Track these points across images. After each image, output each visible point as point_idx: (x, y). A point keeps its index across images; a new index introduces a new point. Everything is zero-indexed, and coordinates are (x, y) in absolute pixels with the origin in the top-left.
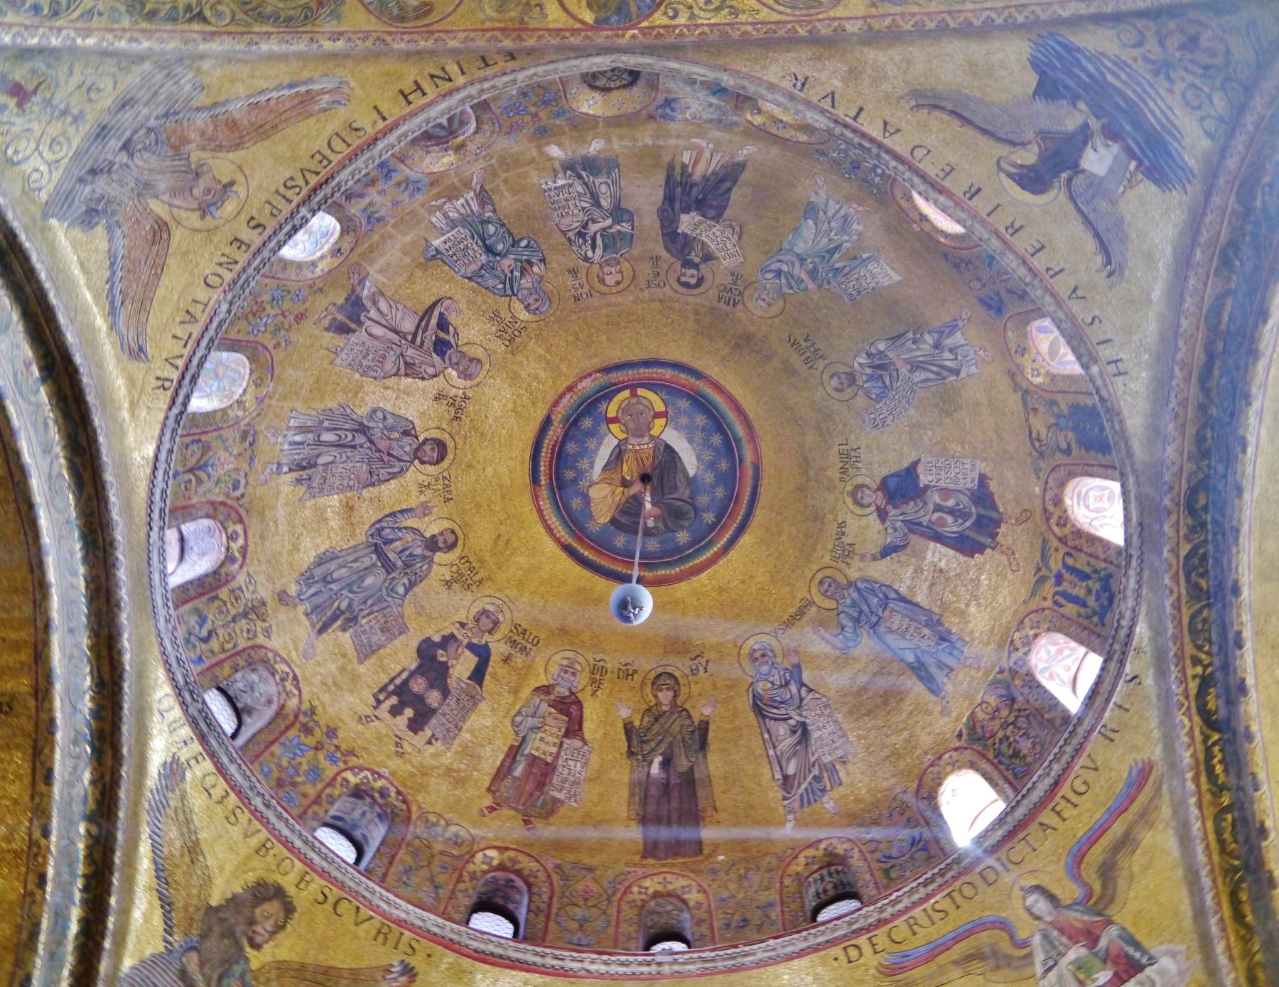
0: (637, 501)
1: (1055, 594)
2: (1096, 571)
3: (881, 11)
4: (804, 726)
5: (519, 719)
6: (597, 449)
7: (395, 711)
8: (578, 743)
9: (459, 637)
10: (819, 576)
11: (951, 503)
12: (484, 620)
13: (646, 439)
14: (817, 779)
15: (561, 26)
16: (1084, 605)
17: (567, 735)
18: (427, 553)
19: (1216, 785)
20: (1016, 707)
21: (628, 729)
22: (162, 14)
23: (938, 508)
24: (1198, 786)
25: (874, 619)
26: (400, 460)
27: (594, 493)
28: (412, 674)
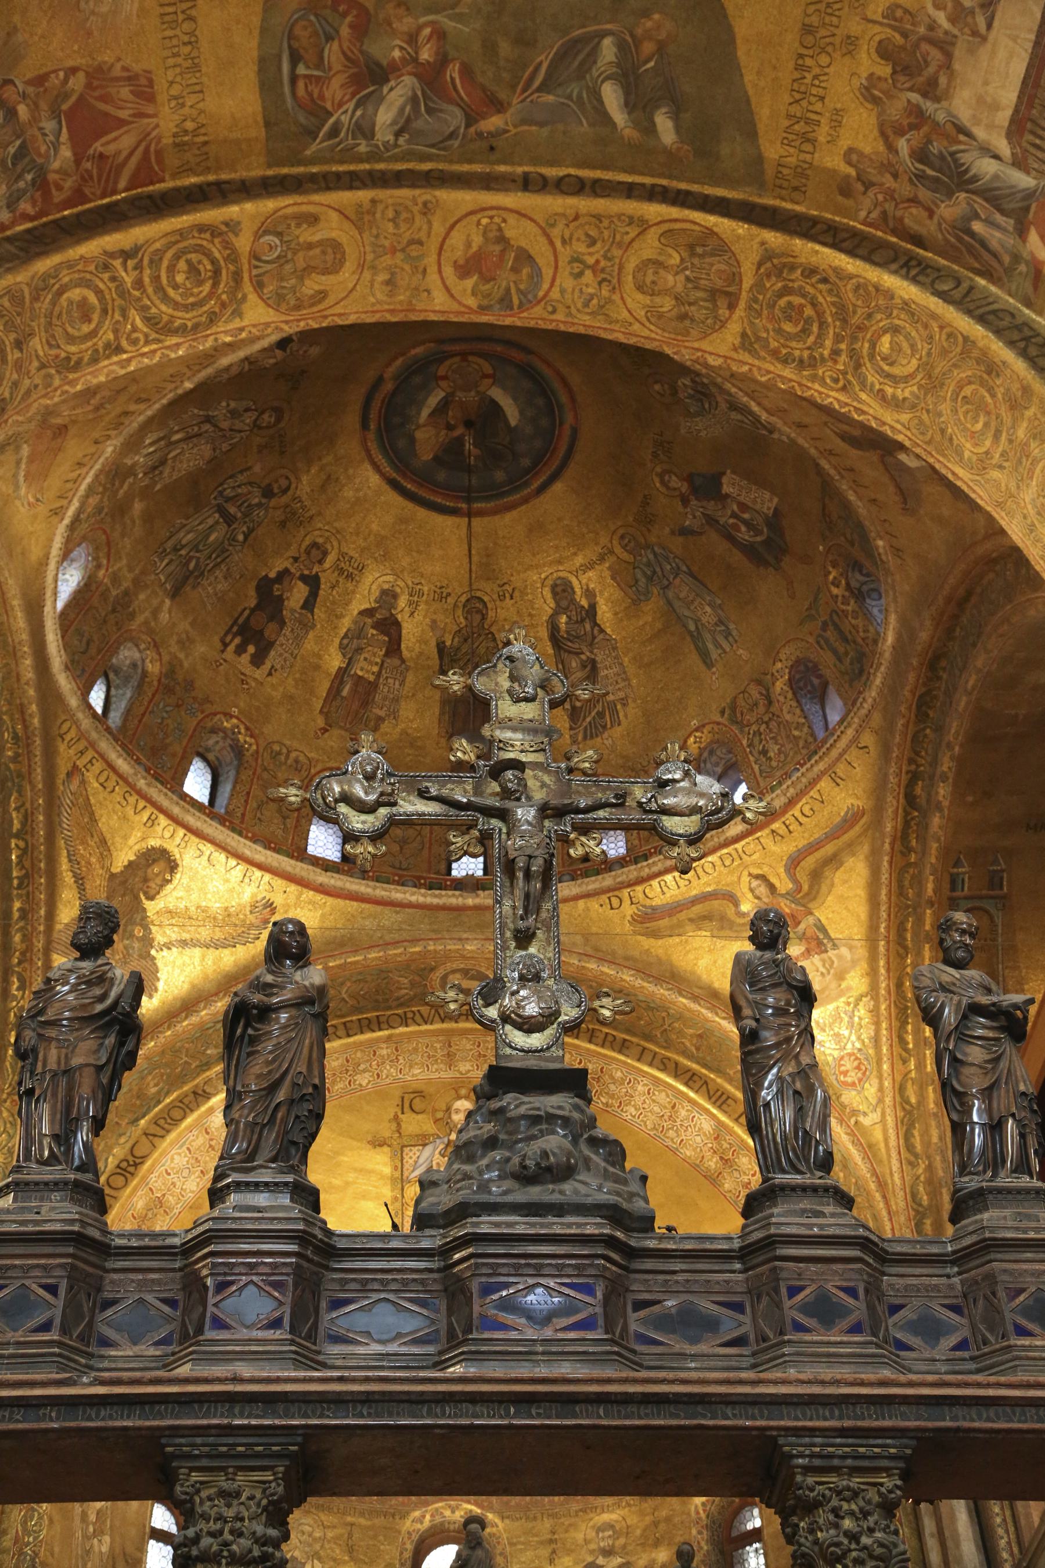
0: (460, 441)
1: (820, 636)
2: (854, 642)
3: (741, 358)
4: (593, 662)
5: (345, 641)
6: (426, 399)
7: (240, 650)
8: (396, 662)
9: (293, 570)
10: (621, 531)
11: (746, 516)
12: (314, 552)
13: (473, 393)
14: (601, 715)
15: (446, 309)
16: (840, 660)
17: (387, 654)
18: (264, 501)
19: (907, 848)
20: (772, 709)
21: (441, 648)
22: (86, 359)
23: (734, 515)
24: (892, 849)
25: (666, 583)
26: (240, 431)
27: (419, 435)
28: (253, 611)
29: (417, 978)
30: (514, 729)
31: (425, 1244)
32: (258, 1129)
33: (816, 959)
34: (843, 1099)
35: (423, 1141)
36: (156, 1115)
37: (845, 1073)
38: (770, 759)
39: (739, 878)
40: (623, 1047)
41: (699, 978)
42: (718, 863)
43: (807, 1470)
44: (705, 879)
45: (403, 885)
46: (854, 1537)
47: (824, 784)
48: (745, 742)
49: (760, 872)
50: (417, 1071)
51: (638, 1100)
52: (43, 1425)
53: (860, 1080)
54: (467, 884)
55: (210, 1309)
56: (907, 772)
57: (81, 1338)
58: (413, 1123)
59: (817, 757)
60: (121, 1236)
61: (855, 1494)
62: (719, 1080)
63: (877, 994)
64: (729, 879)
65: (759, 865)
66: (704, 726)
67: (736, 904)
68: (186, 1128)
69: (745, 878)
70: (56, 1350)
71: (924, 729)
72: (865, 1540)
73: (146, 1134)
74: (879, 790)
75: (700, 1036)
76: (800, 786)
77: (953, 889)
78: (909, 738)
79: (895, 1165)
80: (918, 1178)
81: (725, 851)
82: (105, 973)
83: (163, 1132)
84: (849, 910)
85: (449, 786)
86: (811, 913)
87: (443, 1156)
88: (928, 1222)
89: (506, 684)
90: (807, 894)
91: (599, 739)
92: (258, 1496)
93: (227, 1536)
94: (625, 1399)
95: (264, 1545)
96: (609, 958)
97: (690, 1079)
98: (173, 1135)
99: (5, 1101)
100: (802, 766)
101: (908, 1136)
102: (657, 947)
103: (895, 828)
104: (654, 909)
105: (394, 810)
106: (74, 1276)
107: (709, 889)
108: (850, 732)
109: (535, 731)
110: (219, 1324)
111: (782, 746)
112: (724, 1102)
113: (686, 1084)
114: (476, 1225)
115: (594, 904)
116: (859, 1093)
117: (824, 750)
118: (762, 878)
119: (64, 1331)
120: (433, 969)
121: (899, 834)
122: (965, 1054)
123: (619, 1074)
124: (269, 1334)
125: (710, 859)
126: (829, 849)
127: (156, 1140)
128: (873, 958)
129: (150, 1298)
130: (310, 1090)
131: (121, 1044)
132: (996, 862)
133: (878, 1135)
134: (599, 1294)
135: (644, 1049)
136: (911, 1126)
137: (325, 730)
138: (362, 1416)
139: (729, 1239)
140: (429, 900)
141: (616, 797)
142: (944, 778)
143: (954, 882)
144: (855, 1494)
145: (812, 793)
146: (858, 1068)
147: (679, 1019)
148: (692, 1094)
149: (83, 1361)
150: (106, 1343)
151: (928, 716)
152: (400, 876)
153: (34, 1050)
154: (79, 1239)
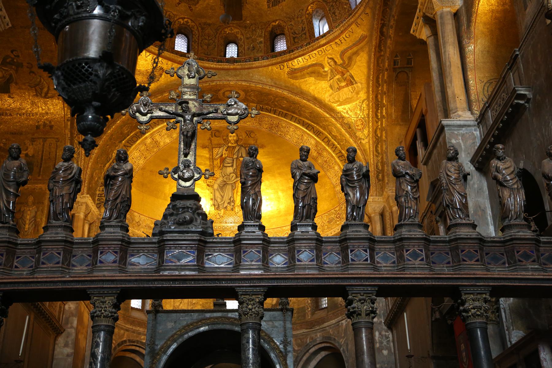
24: (375, 50)
29: (215, 93)
30: (187, 88)
31: (154, 240)
32: (112, 210)
33: (350, 87)
34: (357, 134)
35: (219, 146)
36: (128, 139)
37: (358, 126)
38: (336, 16)
39: (324, 59)
40: (285, 116)
41: (310, 93)
42: (317, 53)
43: (241, 295)
44: (312, 59)
45: (208, 61)
46: (250, 309)
47: (353, 26)
48: (328, 9)
49: (331, 57)
50: (216, 124)
51: (291, 133)
52: (58, 287)
53: (362, 128)
54: (232, 60)
55: (99, 258)
56: (381, 23)
57: (67, 265)
58: (215, 140)
59: (351, 17)
60: (76, 239)
61: (253, 300)
62: (317, 127)
63: (369, 100)
64: (321, 59)
65: (331, 55)
66: (314, 2)
67: (323, 68)
68: (138, 144)
69: (326, 59)
70: (61, 269)
71: (386, 8)
72: (253, 310)
73: (125, 146)
74: (371, 29)
75: (311, 113)
76: (346, 27)
77: (394, 65)
78: (381, 12)
79: (372, 156)
80: (379, 161)
81: (319, 49)
82: (71, 166)
83: (130, 145)
84: (361, 71)
85: (168, 107)
86: (348, 72)
87: (226, 151)
88: (380, 175)
89: (187, 72)
90: (347, 65)
91: (277, 6)
92: (111, 302)
93: (103, 311)
94: (198, 280)
95: (112, 313)
96: (279, 86)
97: (308, 126)
98: (134, 146)
99: (75, 137)
100: (346, 19)
101: (377, 147)
102: (296, 82)
103: (376, 43)
104: (295, 69)
105: (152, 115)
106: (65, 250)
107: (314, 63)
108: (362, 8)
109: (193, 88)
110: (101, 262)
111: (340, 11)
112: (319, 134)
113: (306, 128)
114: (166, 237)
115: (274, 68)
116: (362, 132)
117: (353, 14)
118: (332, 59)
119: (63, 263)
120: (219, 90)
121: (378, 45)
122: (300, 187)
123: (284, 125)
124: (114, 265)
125: (314, 52)
126: (355, 49)
127: (128, 148)
128: (368, 88)
129: (84, 255)
130: (126, 199)
131: (76, 186)
132: (409, 55)
133: (367, 146)
134: (196, 254)
135: (293, 116)
136: (378, 143)
137: (179, 4)
138: (135, 284)
139: (231, 238)
140: (217, 66)
141: (215, 110)
142: (392, 27)
143: (395, 63)
144: (253, 300)
145: (349, 29)
146: (362, 124)
147: (303, 107)
148: (308, 132)
149: (67, 271)
150: (74, 266)
151: (387, 4)
152: (208, 58)
153: (53, 189)
154: (66, 241)
